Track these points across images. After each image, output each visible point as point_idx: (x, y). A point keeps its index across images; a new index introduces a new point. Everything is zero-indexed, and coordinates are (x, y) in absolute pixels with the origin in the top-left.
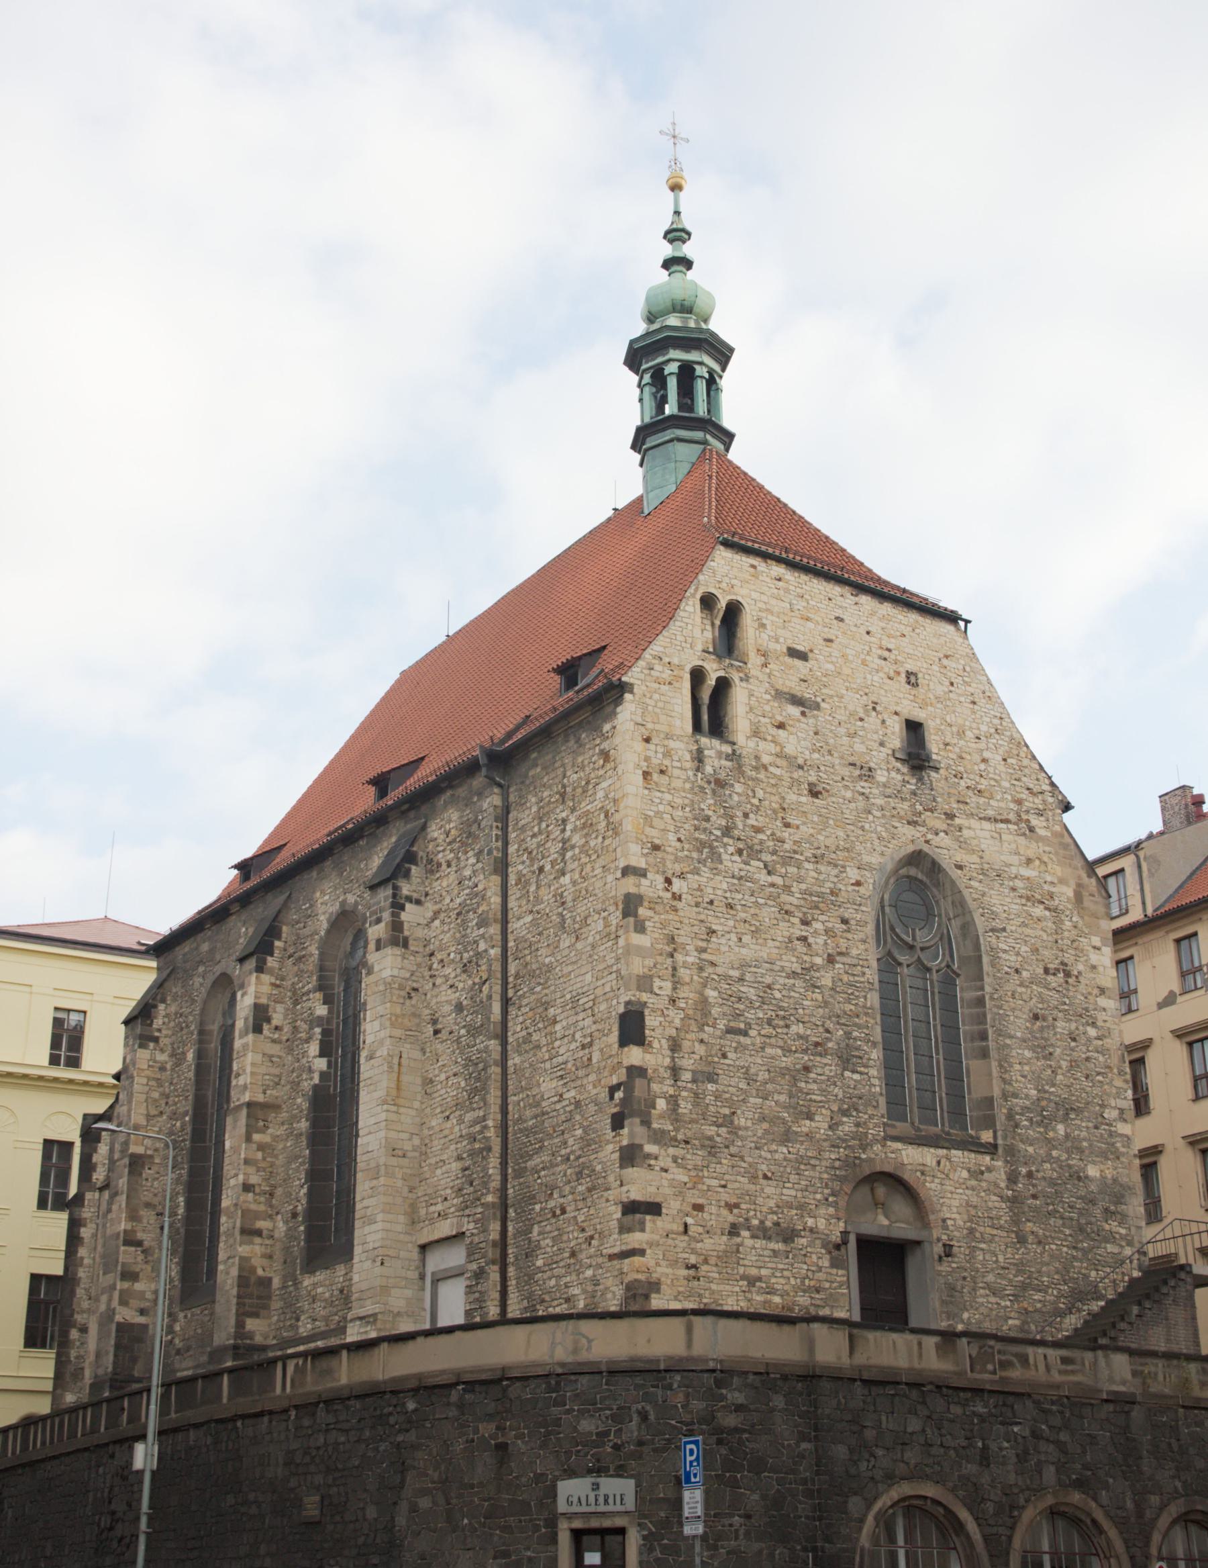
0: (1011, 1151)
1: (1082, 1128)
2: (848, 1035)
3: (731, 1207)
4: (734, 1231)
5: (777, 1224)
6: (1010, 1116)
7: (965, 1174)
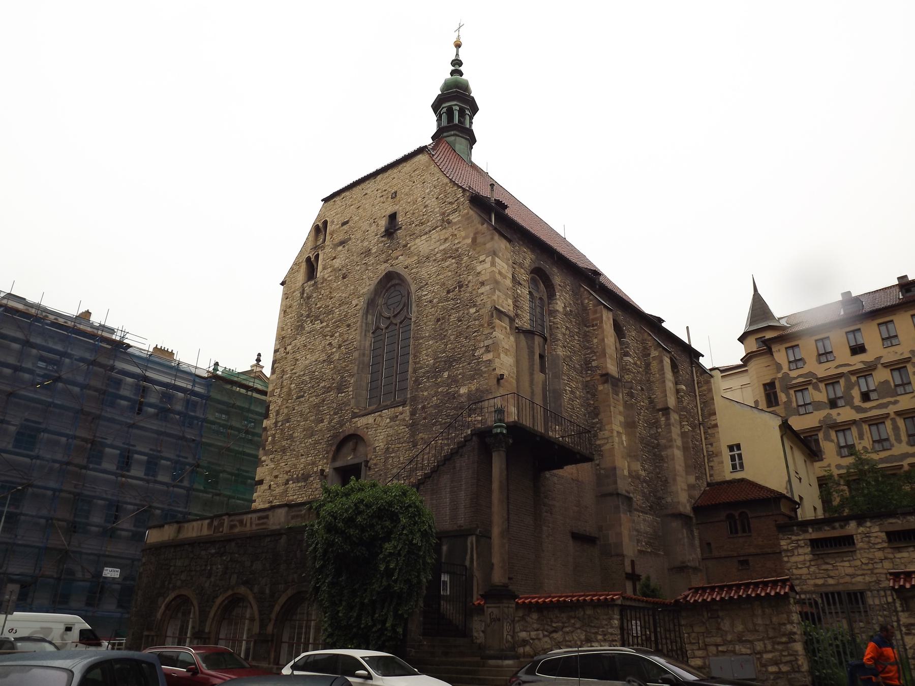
0: (414, 399)
1: (459, 369)
2: (342, 377)
3: (287, 473)
4: (287, 483)
5: (303, 474)
6: (416, 381)
7: (388, 420)
